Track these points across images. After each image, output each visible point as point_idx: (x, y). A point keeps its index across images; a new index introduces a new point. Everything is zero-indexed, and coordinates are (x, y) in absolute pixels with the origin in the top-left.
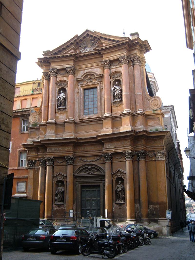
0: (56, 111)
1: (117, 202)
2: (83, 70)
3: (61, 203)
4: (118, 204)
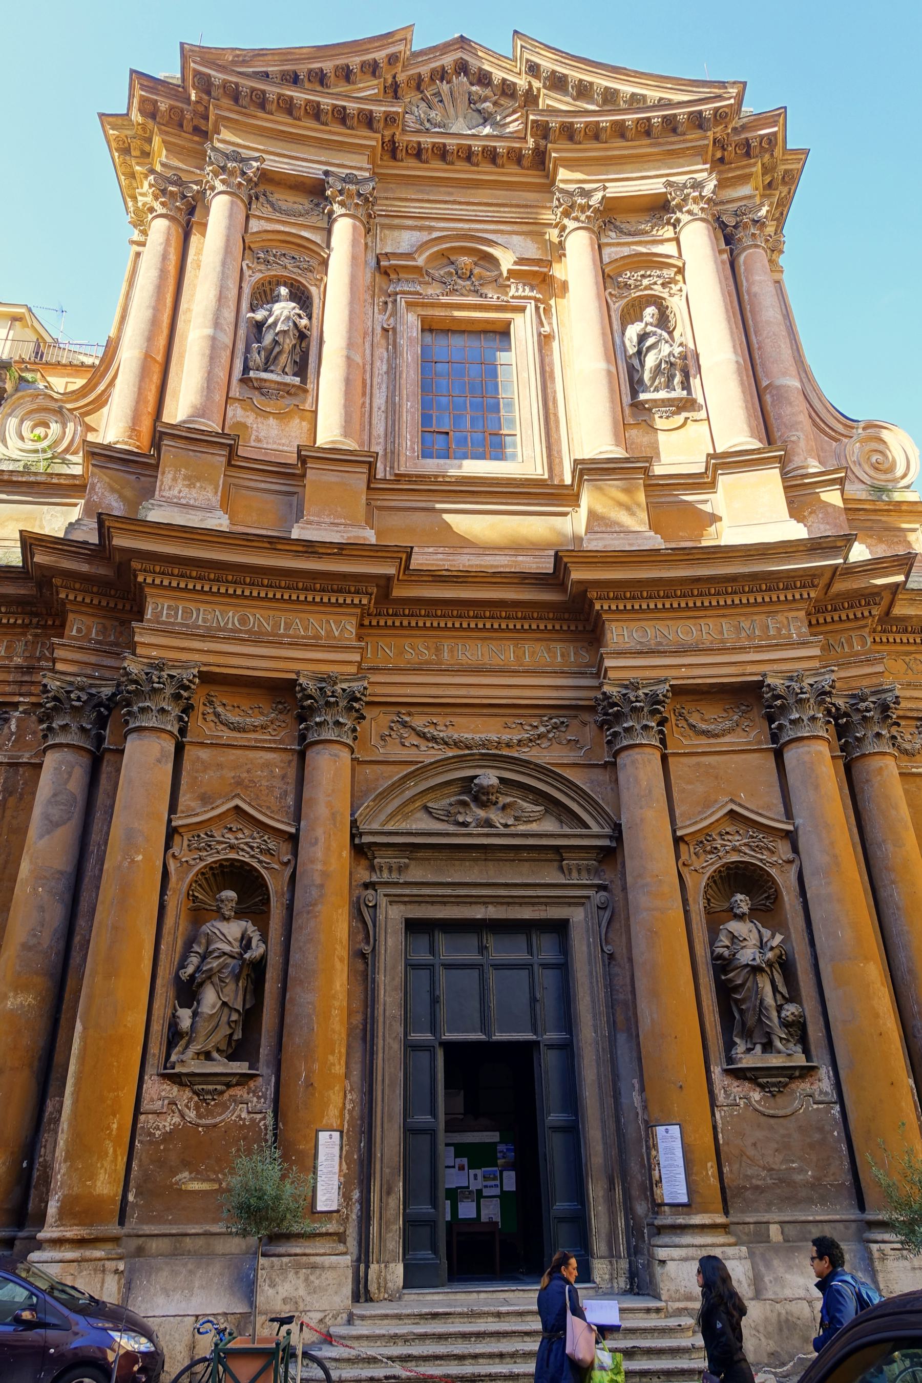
0: (235, 391)
1: (747, 1062)
2: (421, 229)
3: (220, 1066)
4: (754, 1081)
